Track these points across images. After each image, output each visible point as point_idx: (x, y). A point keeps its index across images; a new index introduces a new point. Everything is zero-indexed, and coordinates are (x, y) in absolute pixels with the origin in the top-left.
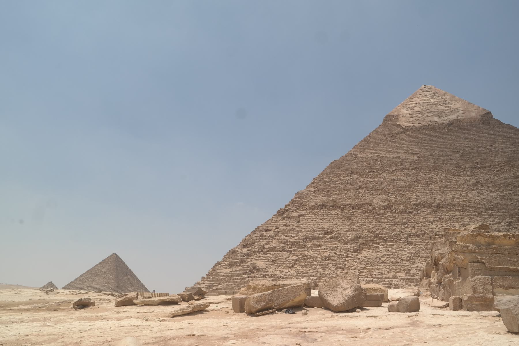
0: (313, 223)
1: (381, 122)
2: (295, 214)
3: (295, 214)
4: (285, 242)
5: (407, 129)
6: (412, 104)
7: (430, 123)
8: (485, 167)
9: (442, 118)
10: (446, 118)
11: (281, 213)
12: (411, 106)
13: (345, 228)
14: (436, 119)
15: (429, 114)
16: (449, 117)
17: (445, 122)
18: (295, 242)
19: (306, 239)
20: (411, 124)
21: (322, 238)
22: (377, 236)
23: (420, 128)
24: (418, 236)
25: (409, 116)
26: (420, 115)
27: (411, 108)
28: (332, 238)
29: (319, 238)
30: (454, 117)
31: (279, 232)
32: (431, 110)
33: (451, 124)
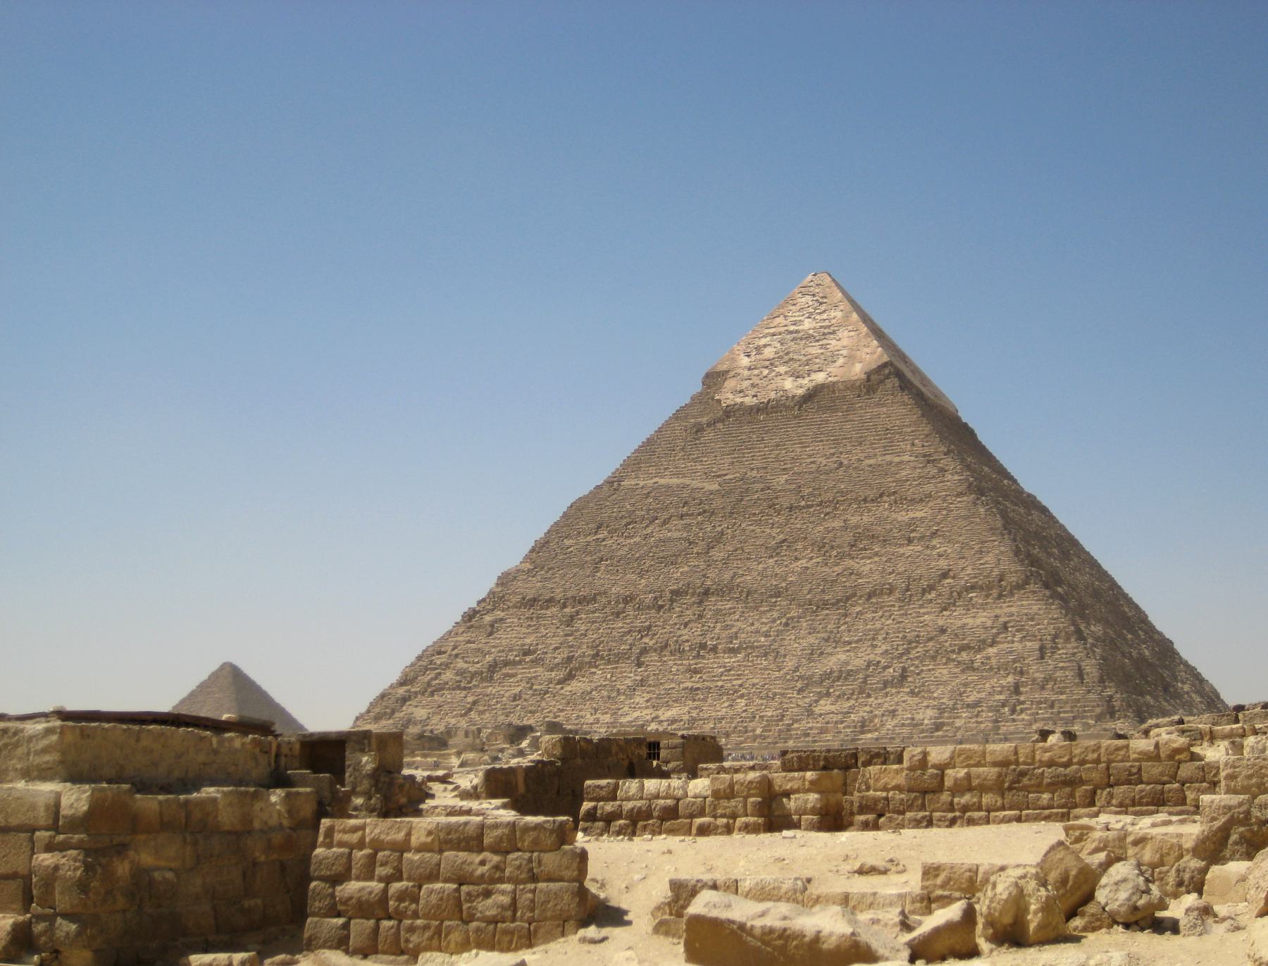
0: (515, 634)
1: (698, 387)
2: (488, 618)
3: (488, 618)
4: (461, 673)
5: (729, 412)
6: (765, 337)
7: (773, 395)
8: (811, 506)
9: (800, 381)
10: (805, 381)
11: (470, 616)
12: (763, 341)
13: (555, 642)
14: (788, 384)
15: (782, 369)
16: (814, 376)
17: (800, 392)
18: (476, 673)
19: (493, 667)
20: (739, 400)
21: (520, 662)
22: (597, 655)
23: (751, 408)
24: (655, 650)
25: (746, 373)
26: (766, 372)
27: (759, 349)
28: (532, 661)
29: (514, 663)
30: (820, 377)
31: (457, 656)
32: (791, 355)
33: (812, 395)
